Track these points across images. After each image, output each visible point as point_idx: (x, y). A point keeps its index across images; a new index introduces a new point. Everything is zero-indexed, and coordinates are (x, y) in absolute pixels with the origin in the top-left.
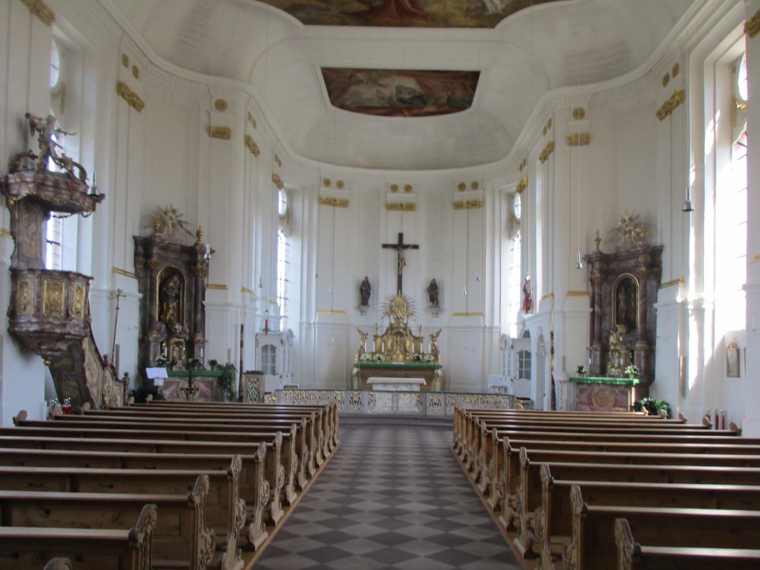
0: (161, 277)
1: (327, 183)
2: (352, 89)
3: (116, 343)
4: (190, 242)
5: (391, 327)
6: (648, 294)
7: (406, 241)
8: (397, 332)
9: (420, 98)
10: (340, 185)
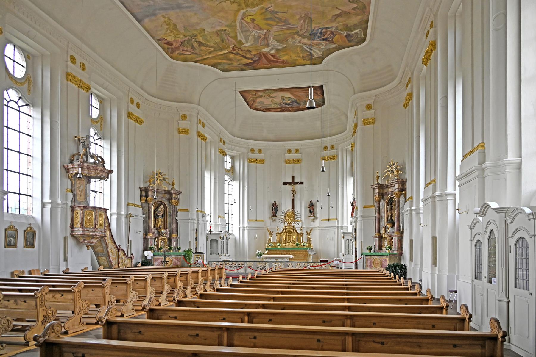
1: (252, 151)
4: (168, 188)
7: (296, 181)
8: (289, 230)
9: (296, 101)
10: (260, 151)
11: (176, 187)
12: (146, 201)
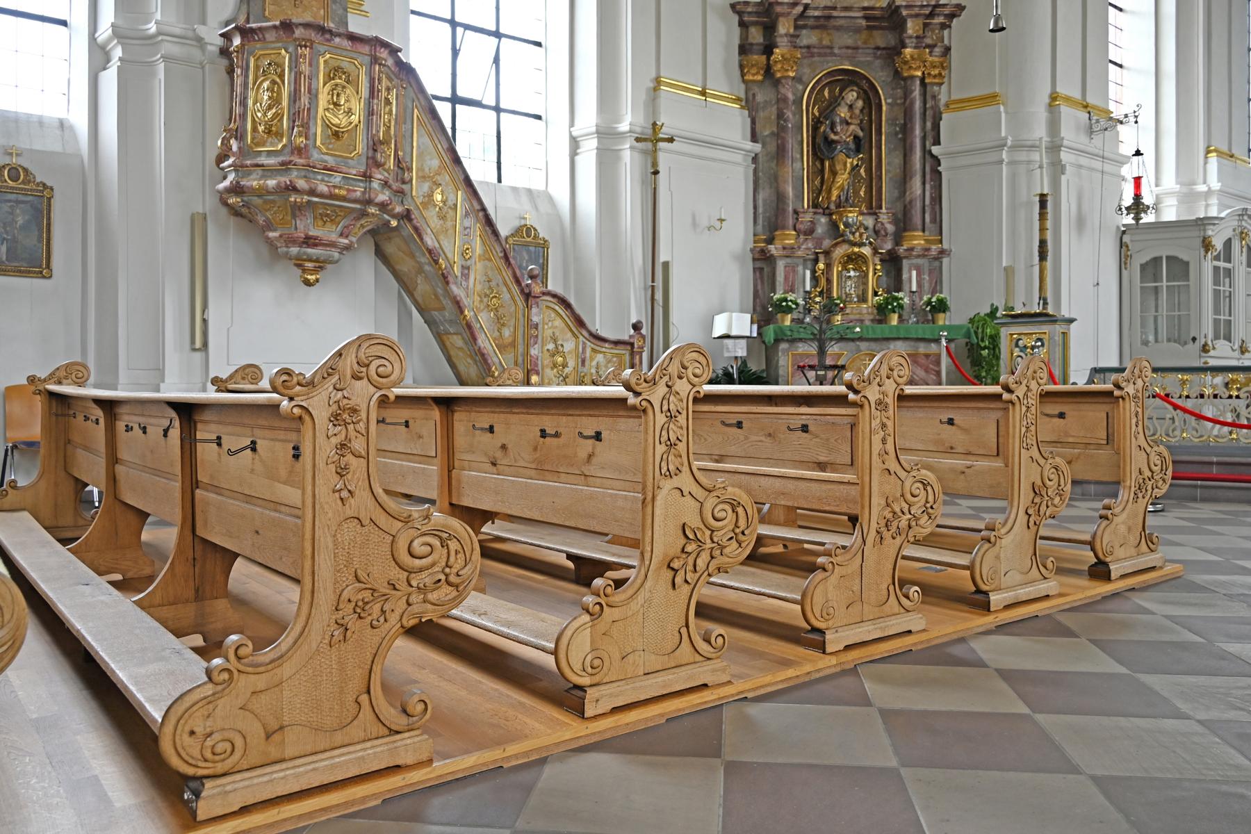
3: (663, 257)
12: (768, 71)
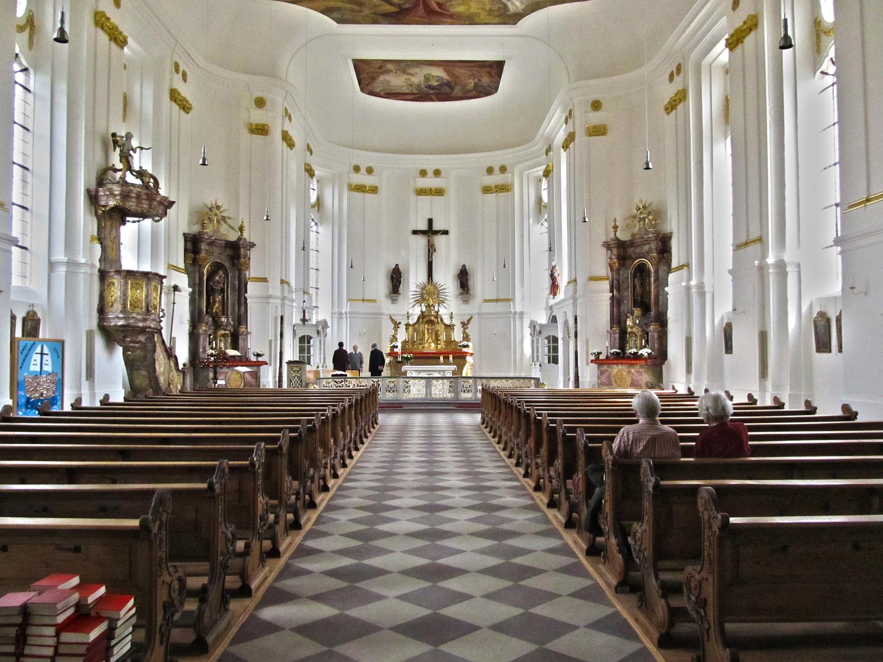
0: (208, 271)
1: (357, 169)
2: (382, 78)
4: (233, 237)
5: (423, 316)
6: (661, 278)
7: (436, 227)
8: (428, 319)
9: (448, 84)
10: (370, 171)
11: (246, 235)
